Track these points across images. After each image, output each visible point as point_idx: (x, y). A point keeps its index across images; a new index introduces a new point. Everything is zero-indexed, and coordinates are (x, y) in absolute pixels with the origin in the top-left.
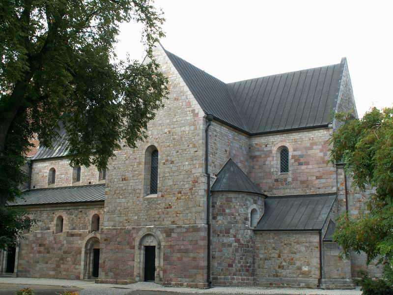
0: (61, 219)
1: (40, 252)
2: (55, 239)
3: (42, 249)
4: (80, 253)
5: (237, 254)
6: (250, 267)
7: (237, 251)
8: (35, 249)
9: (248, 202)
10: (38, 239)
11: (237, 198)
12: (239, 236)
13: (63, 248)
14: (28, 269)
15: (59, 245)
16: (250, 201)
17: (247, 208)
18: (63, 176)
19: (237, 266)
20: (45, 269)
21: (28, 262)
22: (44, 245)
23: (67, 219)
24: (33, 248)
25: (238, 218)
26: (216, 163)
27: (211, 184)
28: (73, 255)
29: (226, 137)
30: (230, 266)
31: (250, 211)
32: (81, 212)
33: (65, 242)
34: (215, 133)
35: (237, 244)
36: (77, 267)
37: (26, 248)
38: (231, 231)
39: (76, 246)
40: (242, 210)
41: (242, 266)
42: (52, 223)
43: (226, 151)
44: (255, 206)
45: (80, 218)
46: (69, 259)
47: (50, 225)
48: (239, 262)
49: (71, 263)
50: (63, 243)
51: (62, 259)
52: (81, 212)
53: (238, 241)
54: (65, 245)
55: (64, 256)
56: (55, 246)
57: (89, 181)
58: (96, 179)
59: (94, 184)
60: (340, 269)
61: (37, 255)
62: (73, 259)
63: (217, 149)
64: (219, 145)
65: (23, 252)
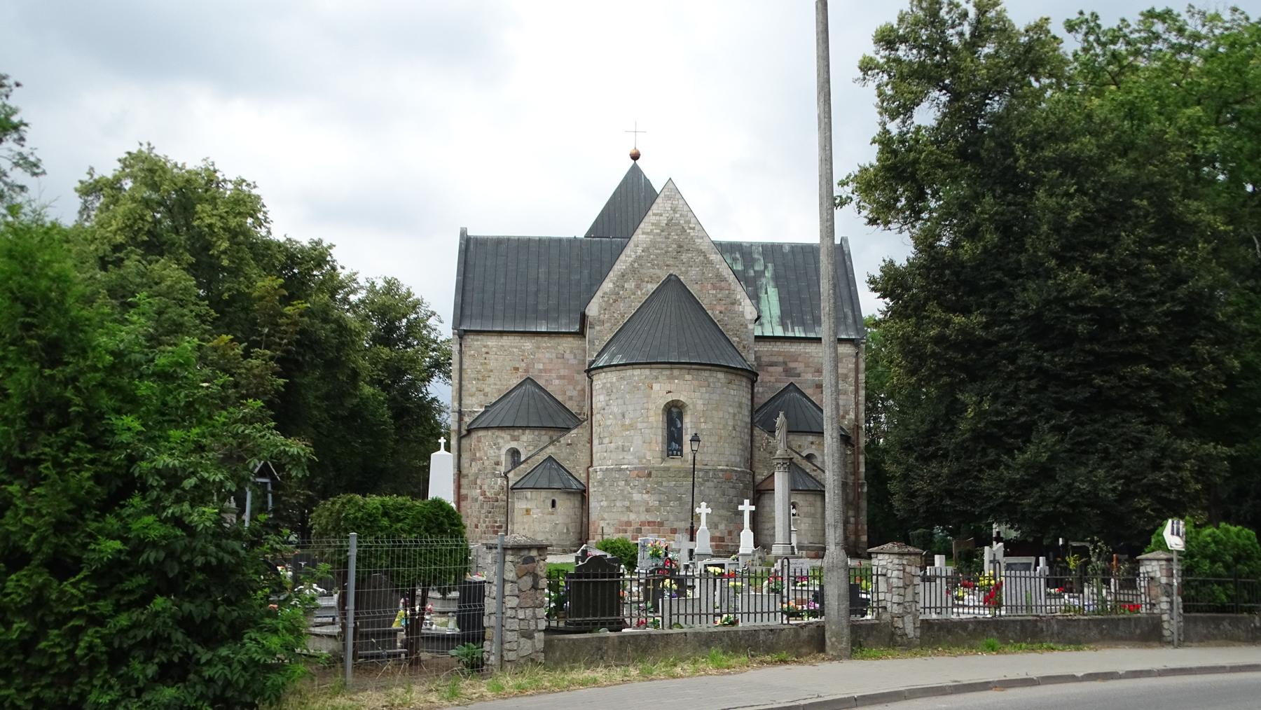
5: (483, 511)
6: (500, 527)
7: (482, 506)
9: (500, 441)
11: (485, 436)
12: (485, 487)
16: (503, 438)
17: (499, 449)
19: (482, 527)
25: (486, 463)
26: (487, 390)
27: (467, 420)
29: (515, 350)
30: (476, 527)
31: (504, 451)
34: (484, 350)
35: (481, 498)
38: (479, 482)
40: (491, 452)
41: (487, 527)
43: (517, 369)
44: (514, 445)
48: (485, 522)
53: (483, 493)
60: (526, 527)
63: (491, 371)
64: (492, 364)
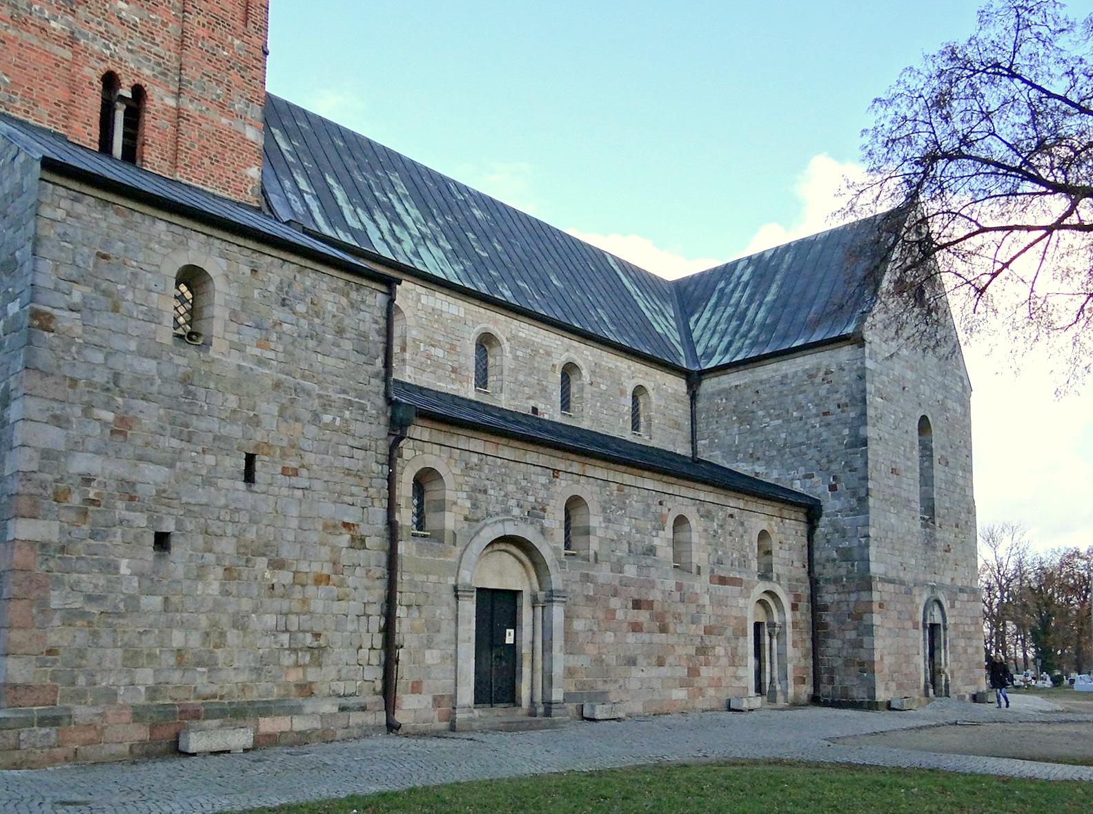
0: (681, 521)
1: (636, 628)
2: (679, 587)
3: (643, 616)
4: (745, 635)
8: (620, 615)
10: (625, 583)
13: (705, 621)
14: (601, 686)
15: (693, 609)
18: (439, 352)
20: (657, 684)
21: (599, 661)
22: (650, 605)
23: (700, 529)
24: (611, 613)
28: (728, 639)
32: (731, 516)
33: (705, 600)
36: (741, 672)
37: (587, 611)
39: (734, 612)
42: (661, 532)
45: (730, 535)
46: (720, 651)
47: (656, 542)
49: (724, 661)
50: (701, 602)
51: (702, 650)
52: (731, 516)
54: (709, 609)
55: (707, 642)
56: (681, 608)
57: (532, 403)
58: (552, 407)
59: (546, 417)
61: (631, 638)
62: (729, 649)
65: (578, 625)
